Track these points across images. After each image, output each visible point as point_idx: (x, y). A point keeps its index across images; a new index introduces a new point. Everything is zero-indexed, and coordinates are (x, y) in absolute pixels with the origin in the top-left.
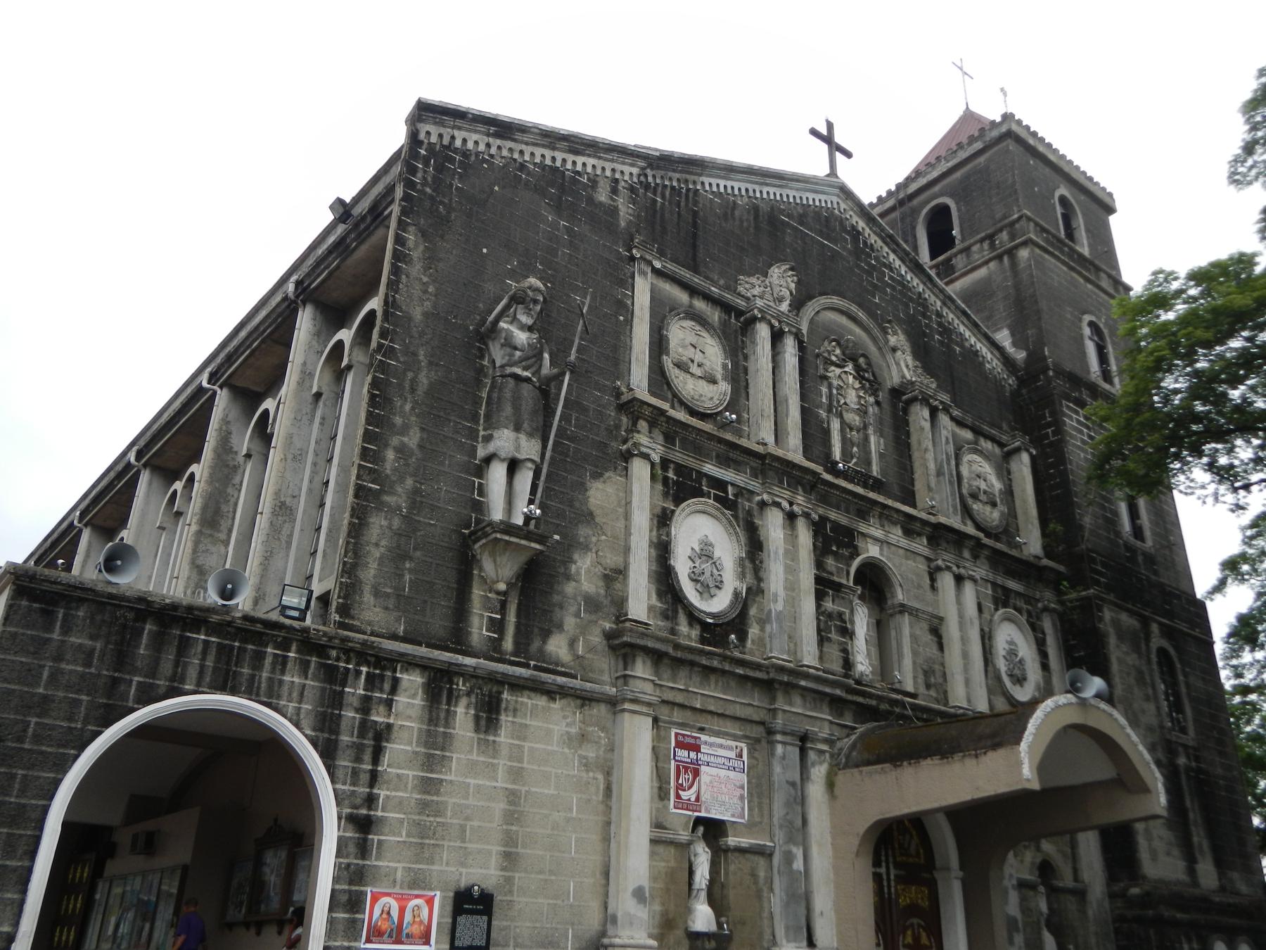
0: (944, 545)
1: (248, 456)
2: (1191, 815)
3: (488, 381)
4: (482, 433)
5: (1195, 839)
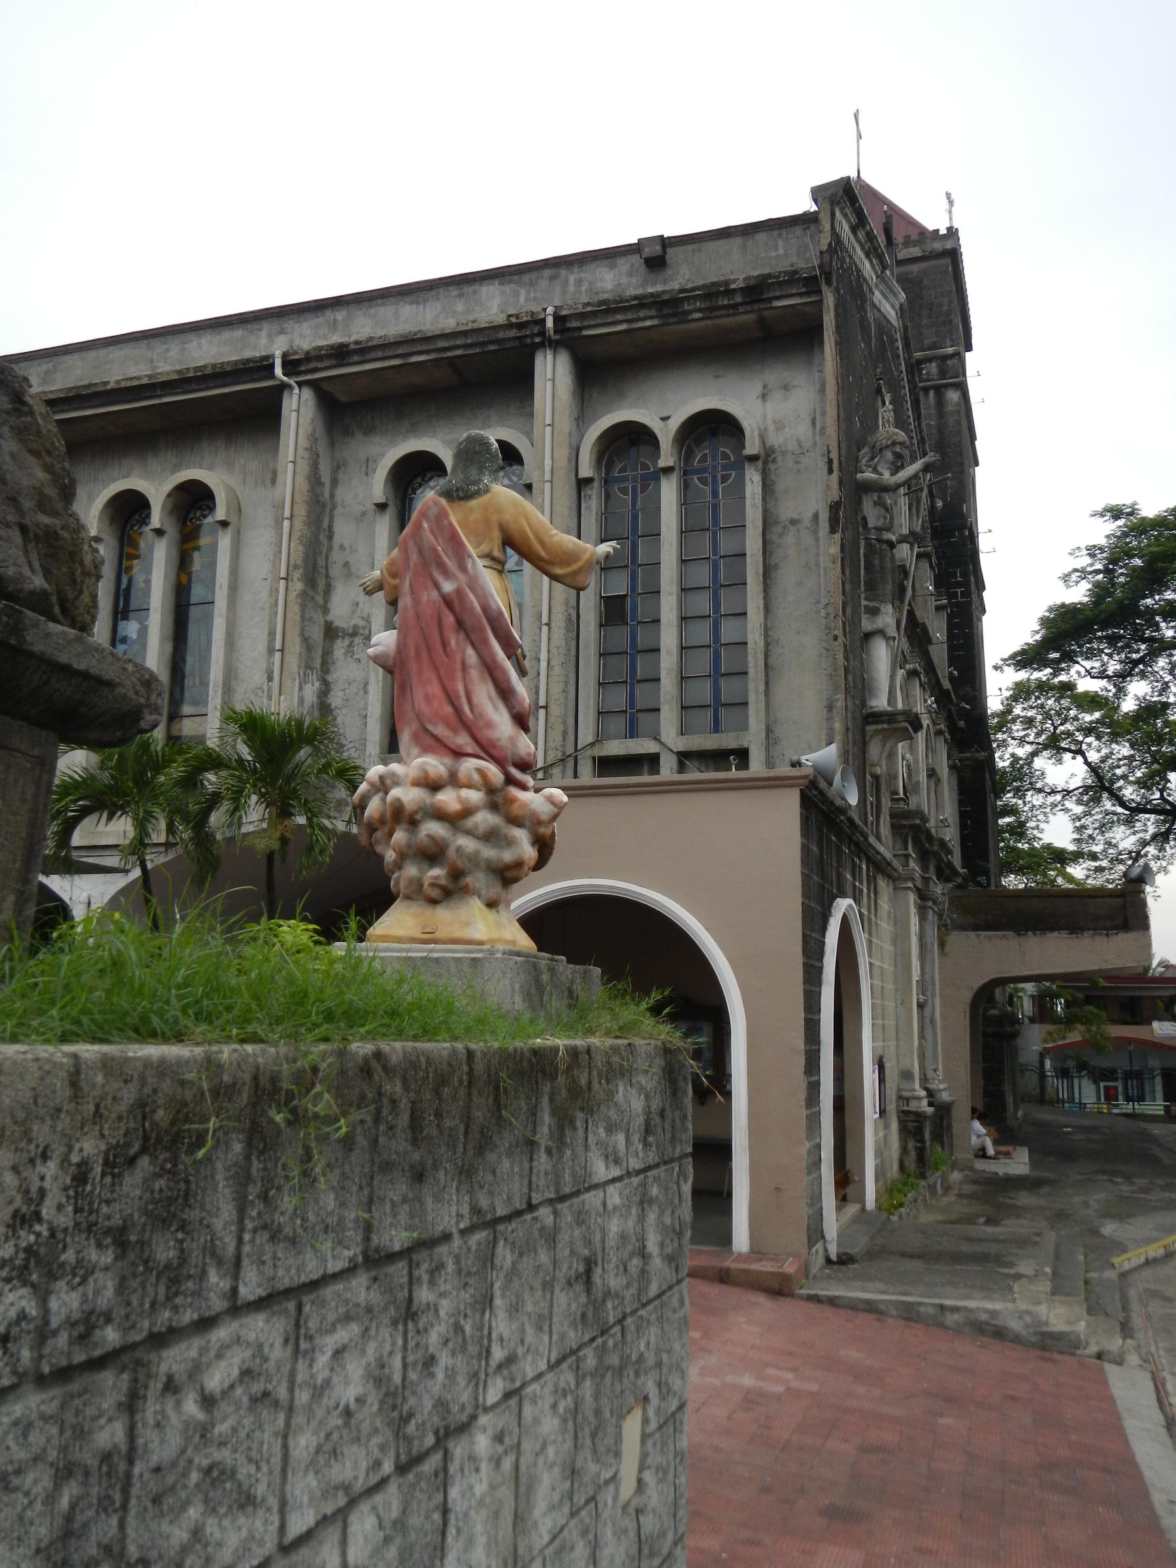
1: (382, 507)
3: (863, 543)
4: (864, 603)
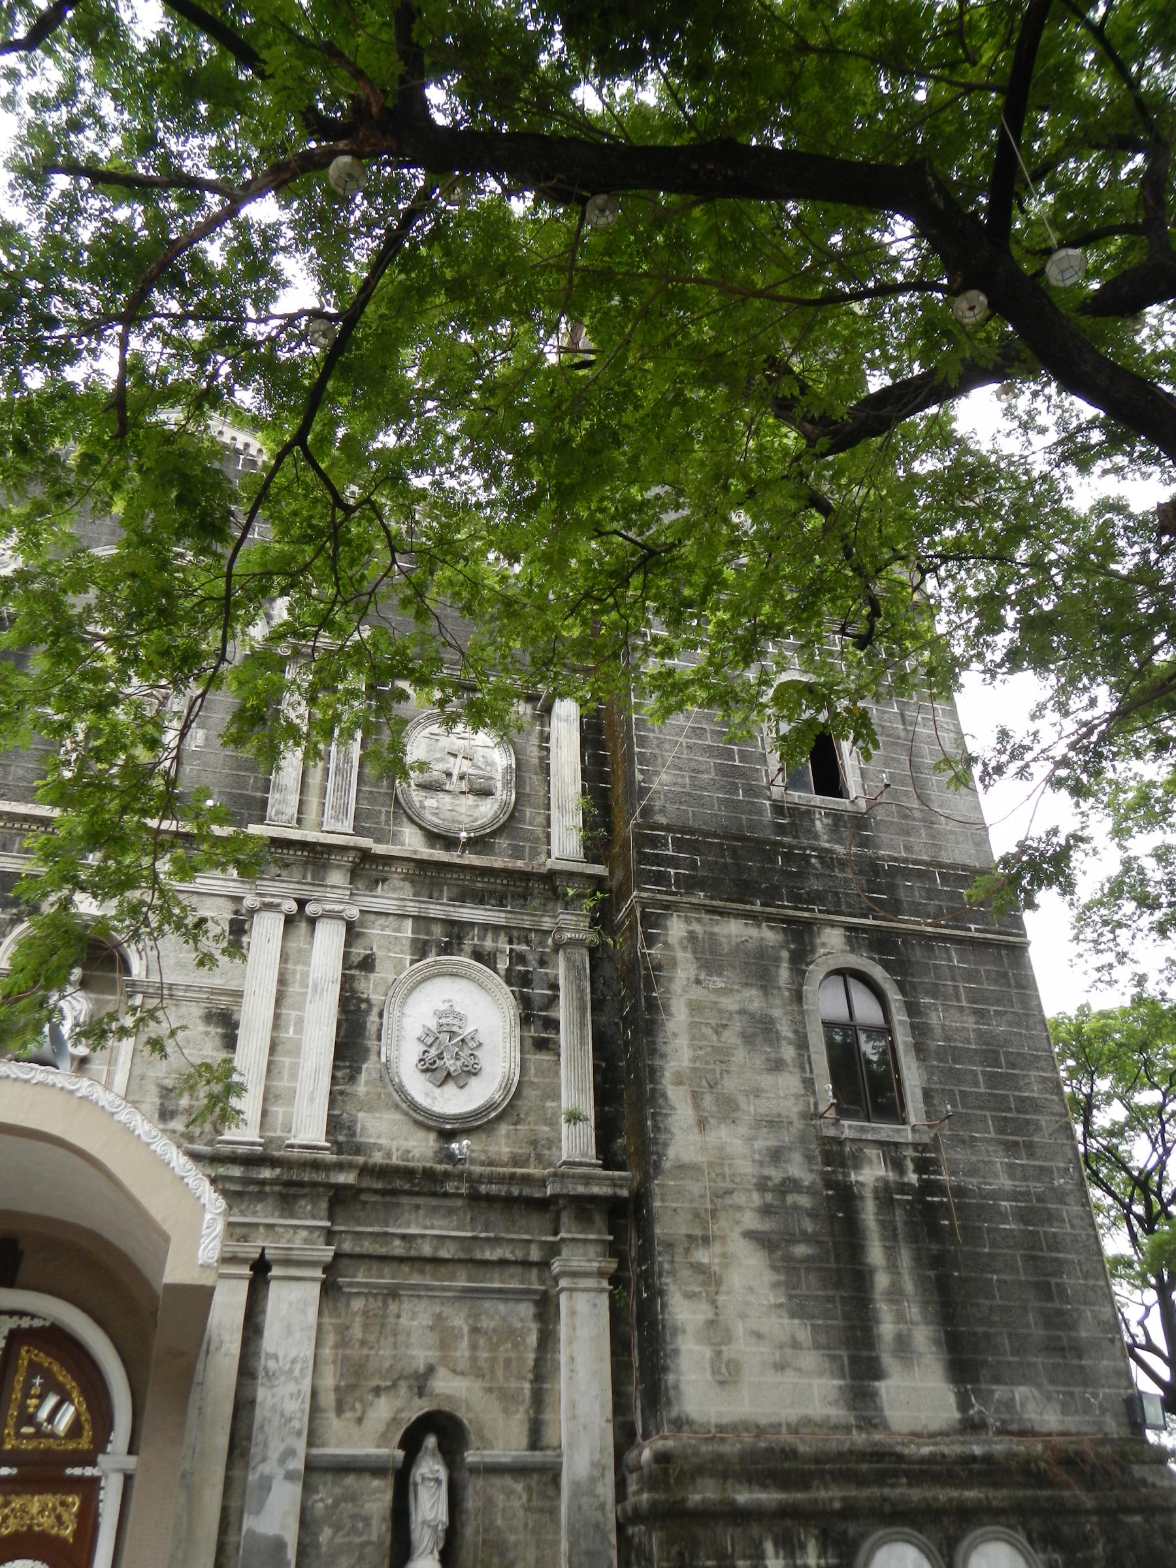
0: (274, 870)
2: (882, 1281)
5: (887, 1329)
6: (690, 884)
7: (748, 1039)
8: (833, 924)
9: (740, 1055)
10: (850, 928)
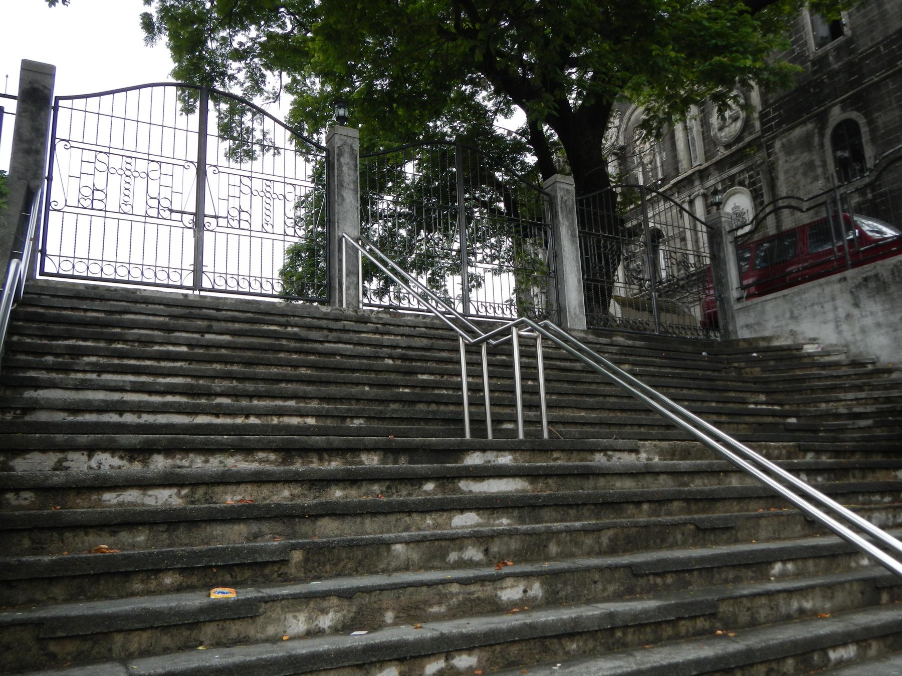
6: (779, 125)
7: (805, 174)
8: (835, 105)
9: (803, 182)
10: (841, 102)
